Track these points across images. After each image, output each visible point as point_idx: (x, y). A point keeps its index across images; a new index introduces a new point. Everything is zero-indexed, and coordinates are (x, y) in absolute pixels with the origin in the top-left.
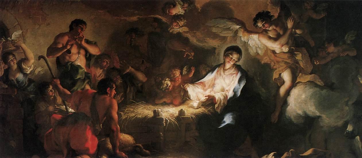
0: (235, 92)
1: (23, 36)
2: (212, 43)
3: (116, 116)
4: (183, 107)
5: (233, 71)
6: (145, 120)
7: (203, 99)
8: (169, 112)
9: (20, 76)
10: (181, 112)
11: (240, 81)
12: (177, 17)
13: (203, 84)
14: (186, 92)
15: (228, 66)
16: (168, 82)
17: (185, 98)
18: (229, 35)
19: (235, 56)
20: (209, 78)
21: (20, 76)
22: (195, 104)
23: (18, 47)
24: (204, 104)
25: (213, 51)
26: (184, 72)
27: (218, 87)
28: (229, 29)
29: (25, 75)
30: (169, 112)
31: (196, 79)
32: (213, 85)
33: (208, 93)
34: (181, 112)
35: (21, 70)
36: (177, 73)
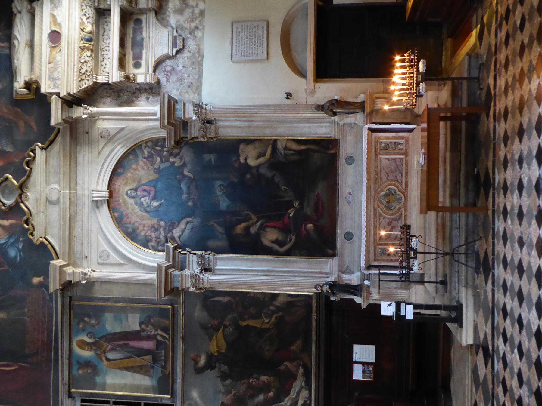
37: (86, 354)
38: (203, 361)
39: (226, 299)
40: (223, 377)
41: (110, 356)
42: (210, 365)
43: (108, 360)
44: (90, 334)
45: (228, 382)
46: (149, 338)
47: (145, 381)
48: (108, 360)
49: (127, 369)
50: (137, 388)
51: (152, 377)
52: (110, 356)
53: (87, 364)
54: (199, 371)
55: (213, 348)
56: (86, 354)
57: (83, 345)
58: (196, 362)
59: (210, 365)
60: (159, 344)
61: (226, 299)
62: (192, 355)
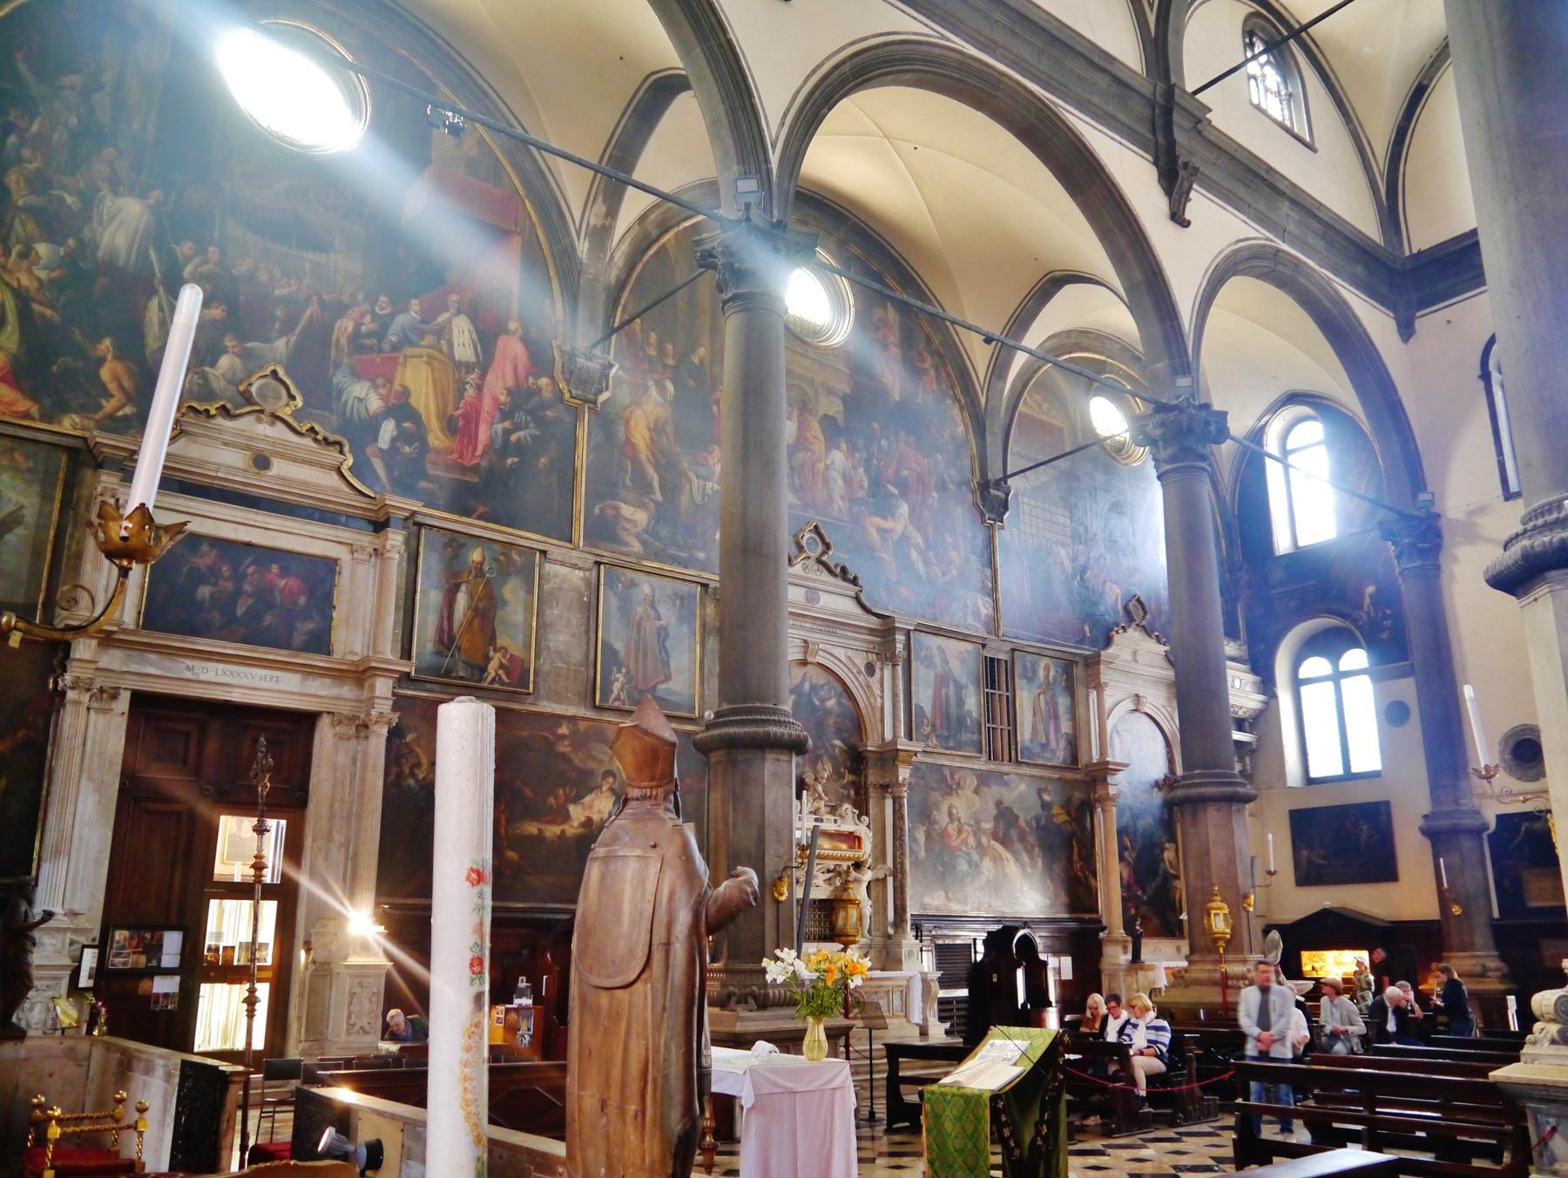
1: (417, 739)
2: (593, 765)
4: (565, 827)
6: (530, 837)
8: (552, 831)
9: (411, 782)
10: (563, 832)
12: (563, 737)
16: (552, 800)
17: (566, 818)
18: (606, 759)
19: (611, 780)
20: (587, 799)
21: (411, 782)
23: (412, 751)
24: (583, 825)
25: (591, 773)
27: (596, 809)
29: (417, 780)
30: (552, 831)
31: (576, 799)
32: (591, 807)
33: (587, 813)
34: (563, 832)
35: (413, 775)
38: (1046, 798)
54: (1040, 792)
56: (1041, 673)
57: (1047, 669)
58: (1045, 790)
59: (1045, 806)
60: (1053, 752)
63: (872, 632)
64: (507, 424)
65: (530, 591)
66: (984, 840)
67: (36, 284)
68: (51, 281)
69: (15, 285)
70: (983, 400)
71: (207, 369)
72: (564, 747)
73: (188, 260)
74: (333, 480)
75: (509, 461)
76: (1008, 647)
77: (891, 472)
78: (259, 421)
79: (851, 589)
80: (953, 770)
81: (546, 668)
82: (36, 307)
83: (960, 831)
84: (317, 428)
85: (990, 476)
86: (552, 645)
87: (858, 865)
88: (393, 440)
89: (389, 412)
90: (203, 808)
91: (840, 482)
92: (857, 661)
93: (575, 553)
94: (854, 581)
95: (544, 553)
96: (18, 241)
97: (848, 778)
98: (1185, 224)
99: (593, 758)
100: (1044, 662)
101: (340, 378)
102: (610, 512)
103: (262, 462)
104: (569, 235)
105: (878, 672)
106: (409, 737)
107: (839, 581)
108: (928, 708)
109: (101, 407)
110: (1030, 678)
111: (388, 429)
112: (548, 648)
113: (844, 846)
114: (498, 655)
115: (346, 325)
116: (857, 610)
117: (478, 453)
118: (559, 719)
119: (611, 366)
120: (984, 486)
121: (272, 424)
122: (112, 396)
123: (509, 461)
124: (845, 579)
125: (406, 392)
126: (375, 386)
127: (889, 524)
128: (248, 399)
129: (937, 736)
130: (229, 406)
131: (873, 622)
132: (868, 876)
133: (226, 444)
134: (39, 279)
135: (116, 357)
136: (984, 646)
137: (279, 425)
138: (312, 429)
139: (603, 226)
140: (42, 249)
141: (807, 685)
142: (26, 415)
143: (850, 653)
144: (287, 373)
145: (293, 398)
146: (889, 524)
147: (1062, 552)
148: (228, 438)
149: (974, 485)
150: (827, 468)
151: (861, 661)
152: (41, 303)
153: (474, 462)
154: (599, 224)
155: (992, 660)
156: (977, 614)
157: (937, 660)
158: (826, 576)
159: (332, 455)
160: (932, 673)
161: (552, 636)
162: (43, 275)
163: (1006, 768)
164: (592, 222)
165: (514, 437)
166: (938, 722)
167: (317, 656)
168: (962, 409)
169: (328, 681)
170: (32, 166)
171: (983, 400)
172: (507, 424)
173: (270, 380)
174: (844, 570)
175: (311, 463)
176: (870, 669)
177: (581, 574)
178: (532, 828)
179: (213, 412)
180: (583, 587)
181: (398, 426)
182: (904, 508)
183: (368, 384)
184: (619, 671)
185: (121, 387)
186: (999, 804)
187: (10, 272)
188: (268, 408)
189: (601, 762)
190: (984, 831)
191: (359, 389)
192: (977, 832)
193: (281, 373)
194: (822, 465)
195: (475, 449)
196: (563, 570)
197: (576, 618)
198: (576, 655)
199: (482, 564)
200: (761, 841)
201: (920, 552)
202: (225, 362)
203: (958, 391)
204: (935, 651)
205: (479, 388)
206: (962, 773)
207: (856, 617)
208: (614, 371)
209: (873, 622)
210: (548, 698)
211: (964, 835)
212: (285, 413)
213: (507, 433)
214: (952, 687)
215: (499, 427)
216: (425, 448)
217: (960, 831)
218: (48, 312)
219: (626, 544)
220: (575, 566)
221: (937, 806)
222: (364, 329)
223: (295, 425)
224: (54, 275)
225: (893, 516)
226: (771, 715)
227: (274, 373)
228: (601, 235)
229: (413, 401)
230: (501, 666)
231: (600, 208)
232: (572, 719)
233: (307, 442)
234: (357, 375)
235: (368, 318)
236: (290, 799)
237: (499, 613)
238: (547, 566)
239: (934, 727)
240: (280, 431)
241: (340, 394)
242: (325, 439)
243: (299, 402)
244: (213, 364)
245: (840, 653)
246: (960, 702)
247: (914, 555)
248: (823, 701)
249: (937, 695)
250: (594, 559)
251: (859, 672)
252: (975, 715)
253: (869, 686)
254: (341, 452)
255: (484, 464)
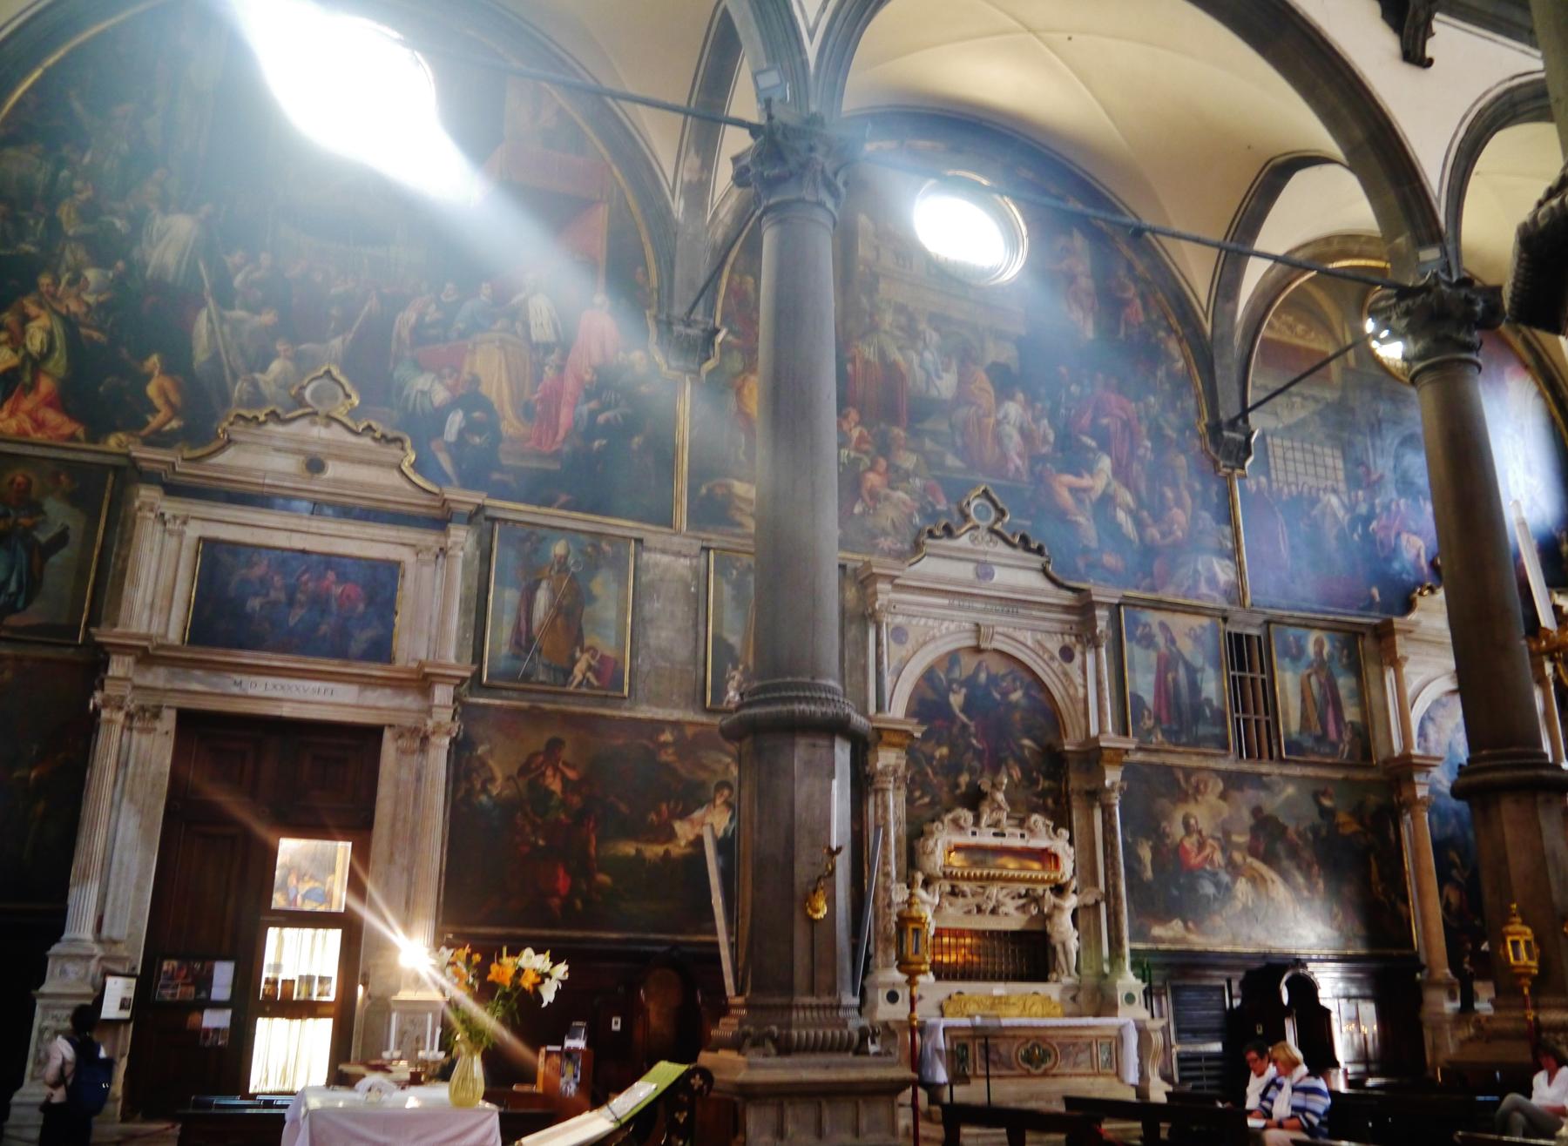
0: (726, 831)
1: (491, 752)
2: (703, 775)
3: (593, 851)
4: (670, 846)
5: (723, 808)
6: (627, 859)
7: (691, 837)
8: (654, 851)
9: (484, 798)
10: (667, 852)
11: (731, 819)
12: (665, 745)
13: (692, 822)
14: (673, 829)
15: (719, 802)
16: (653, 817)
17: (671, 836)
18: (719, 768)
20: (697, 814)
21: (484, 798)
22: (683, 843)
23: (483, 764)
25: (702, 785)
26: (672, 805)
28: (719, 761)
29: (490, 797)
30: (654, 851)
31: (684, 814)
33: (697, 830)
34: (667, 852)
35: (484, 790)
36: (664, 807)
37: (1311, 649)
38: (1327, 803)
39: (1392, 836)
40: (1315, 830)
41: (1313, 680)
42: (1325, 812)
43: (1309, 676)
44: (1331, 656)
45: (1310, 836)
46: (1339, 733)
47: (1295, 726)
48: (1309, 676)
49: (1303, 700)
50: (1286, 714)
51: (1301, 733)
52: (1313, 680)
53: (1301, 650)
54: (1316, 796)
55: (1342, 817)
56: (1311, 649)
57: (1319, 644)
58: (1325, 793)
59: (1325, 812)
60: (1334, 746)
61: (1392, 836)
62: (1330, 790)
63: (1067, 609)
64: (593, 404)
65: (624, 584)
66: (1238, 856)
67: (84, 309)
68: (100, 305)
69: (64, 311)
70: (1208, 327)
71: (257, 376)
72: (667, 756)
73: (238, 269)
74: (394, 479)
75: (596, 444)
76: (1260, 619)
77: (1086, 421)
78: (314, 423)
79: (1036, 561)
80: (1188, 772)
81: (646, 668)
82: (83, 331)
83: (1201, 846)
84: (374, 425)
85: (1224, 416)
86: (652, 642)
87: (1059, 890)
88: (461, 433)
89: (454, 404)
90: (261, 830)
91: (1016, 437)
92: (1049, 645)
93: (676, 539)
94: (1040, 551)
95: (639, 541)
96: (68, 270)
97: (1043, 784)
98: (1427, 63)
99: (705, 768)
100: (1313, 636)
101: (401, 372)
102: (719, 491)
103: (315, 466)
104: (663, 195)
105: (1078, 659)
106: (481, 750)
107: (1020, 553)
108: (1149, 698)
109: (147, 423)
110: (1297, 655)
111: (455, 421)
112: (647, 645)
113: (1036, 865)
114: (586, 656)
115: (409, 316)
116: (1049, 586)
117: (560, 437)
118: (658, 725)
119: (716, 331)
120: (1215, 429)
121: (327, 426)
122: (158, 411)
123: (596, 444)
124: (1028, 549)
125: (476, 380)
126: (440, 378)
127: (1086, 481)
128: (299, 401)
129: (1164, 732)
130: (279, 411)
131: (1067, 598)
132: (1071, 902)
133: (278, 450)
134: (88, 305)
135: (164, 372)
136: (1225, 620)
137: (336, 427)
138: (369, 427)
139: (700, 180)
140: (91, 274)
141: (983, 677)
142: (72, 437)
143: (1039, 636)
144: (344, 372)
145: (348, 396)
146: (1086, 481)
147: (1334, 500)
148: (279, 443)
149: (1202, 428)
150: (998, 423)
151: (1054, 645)
152: (89, 327)
153: (554, 448)
154: (695, 179)
155: (1239, 636)
156: (1212, 581)
157: (1160, 640)
158: (1002, 548)
159: (394, 450)
160: (1153, 656)
161: (652, 633)
162: (91, 299)
163: (1264, 768)
164: (686, 178)
165: (601, 419)
166: (1164, 714)
167: (373, 665)
168: (1180, 341)
169: (388, 691)
170: (83, 197)
171: (1208, 327)
172: (593, 404)
173: (326, 381)
174: (1024, 539)
175: (369, 463)
176: (1067, 654)
177: (687, 562)
178: (629, 849)
179: (262, 418)
180: (689, 576)
181: (466, 416)
182: (1105, 463)
183: (433, 376)
184: (735, 668)
185: (168, 402)
186: (1257, 811)
187: (60, 300)
188: (321, 410)
189: (714, 772)
190: (1238, 847)
191: (422, 382)
192: (1226, 846)
193: (335, 372)
194: (992, 421)
195: (556, 433)
196: (665, 559)
197: (681, 611)
198: (682, 653)
199: (566, 557)
200: (790, 844)
201: (1129, 512)
202: (276, 367)
203: (1173, 321)
204: (1156, 630)
205: (561, 369)
206: (1204, 775)
207: (1041, 592)
208: (720, 337)
209: (1067, 598)
210: (649, 702)
211: (1208, 851)
212: (340, 412)
213: (593, 415)
214: (1182, 672)
215: (585, 409)
216: (497, 437)
217: (1201, 846)
218: (96, 335)
219: (740, 525)
220: (678, 554)
221: (1167, 817)
222: (427, 319)
223: (351, 424)
224: (101, 298)
225: (1091, 473)
226: (811, 691)
227: (328, 372)
228: (698, 192)
229: (483, 389)
230: (590, 667)
231: (693, 161)
232: (676, 725)
233: (366, 441)
234: (420, 368)
235: (433, 307)
236: (353, 819)
237: (587, 610)
238: (645, 556)
239: (1158, 719)
240: (335, 433)
241: (401, 389)
242: (383, 436)
243: (356, 401)
244: (264, 369)
245: (1028, 637)
246: (1195, 688)
247: (1121, 516)
248: (1005, 694)
249: (1161, 685)
250: (700, 544)
251: (1052, 658)
252: (1215, 703)
253: (1066, 674)
254: (403, 449)
255: (567, 448)
